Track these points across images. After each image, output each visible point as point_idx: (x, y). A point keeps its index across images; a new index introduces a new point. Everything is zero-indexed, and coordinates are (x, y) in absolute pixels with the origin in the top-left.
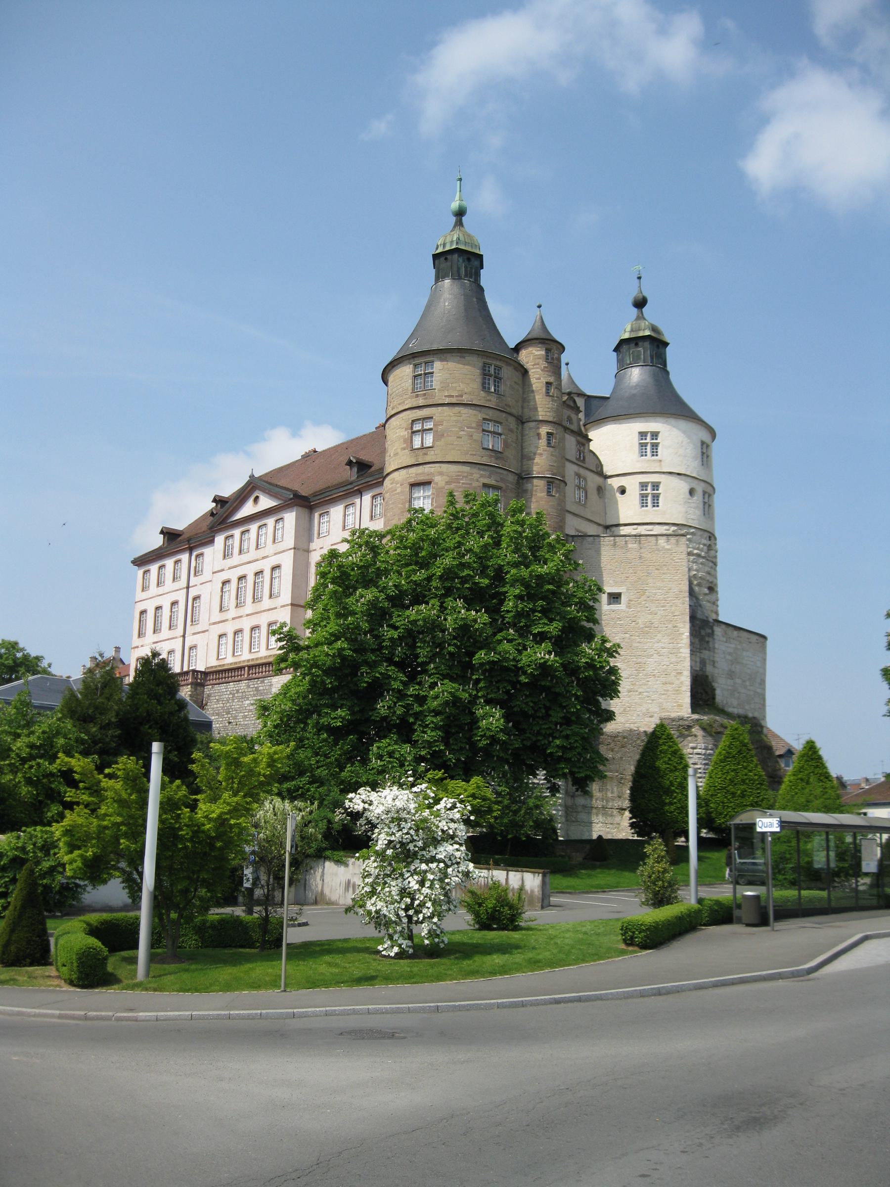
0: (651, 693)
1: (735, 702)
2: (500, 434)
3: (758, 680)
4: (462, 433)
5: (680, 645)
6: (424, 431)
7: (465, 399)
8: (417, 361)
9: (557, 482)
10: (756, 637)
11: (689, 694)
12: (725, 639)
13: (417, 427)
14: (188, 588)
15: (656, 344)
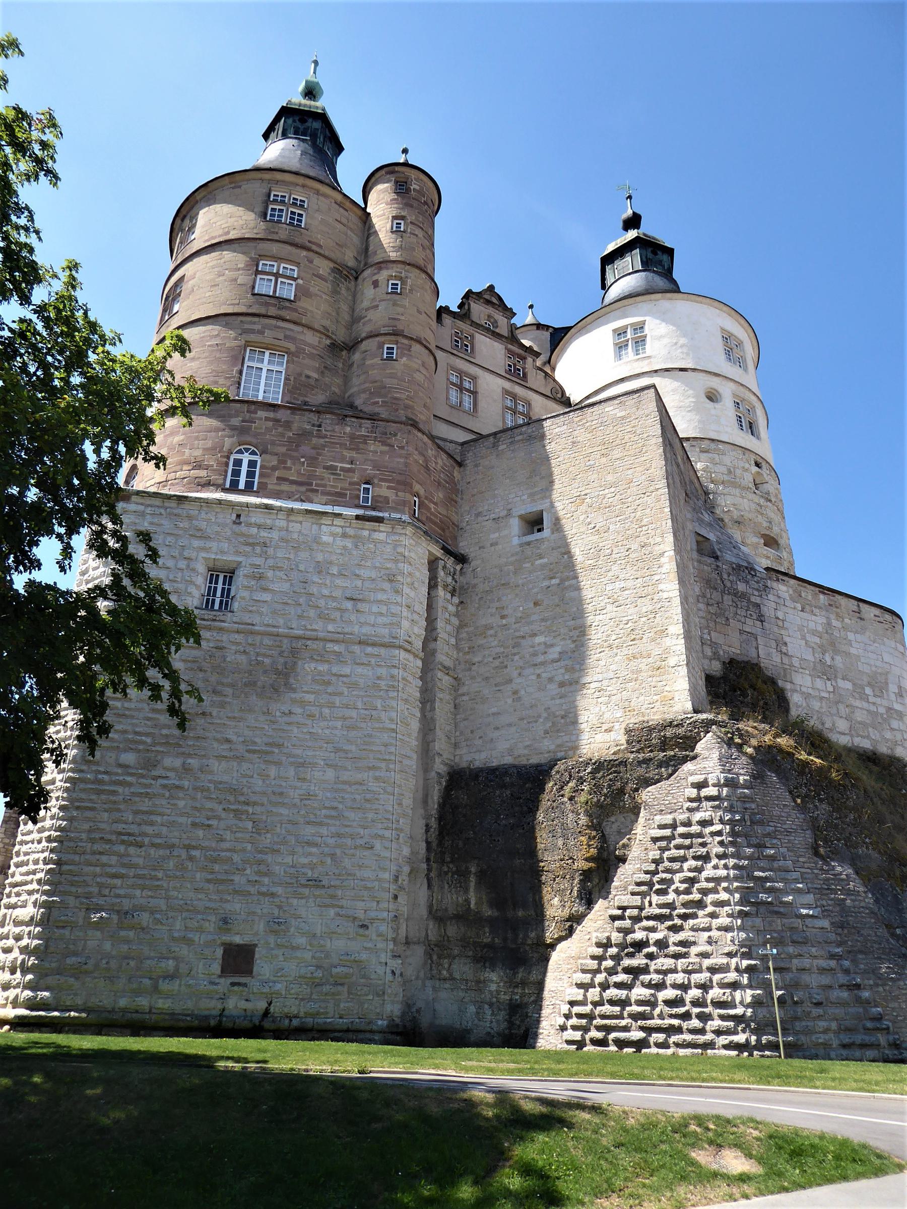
0: (605, 683)
1: (842, 725)
2: (295, 279)
3: (893, 688)
4: (221, 278)
5: (656, 577)
7: (232, 236)
9: (406, 341)
10: (877, 612)
11: (684, 671)
12: (799, 606)
15: (650, 250)
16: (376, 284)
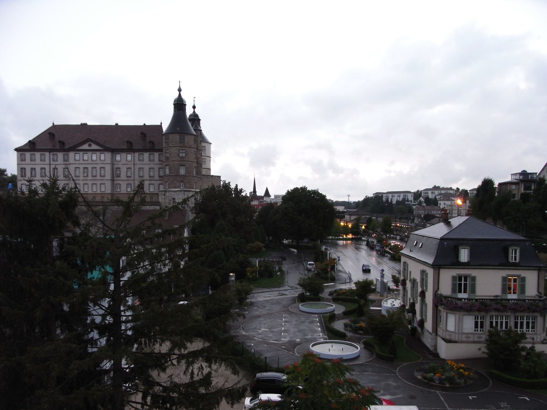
6: (182, 152)
8: (181, 135)
13: (180, 151)
14: (50, 164)
16: (199, 153)
